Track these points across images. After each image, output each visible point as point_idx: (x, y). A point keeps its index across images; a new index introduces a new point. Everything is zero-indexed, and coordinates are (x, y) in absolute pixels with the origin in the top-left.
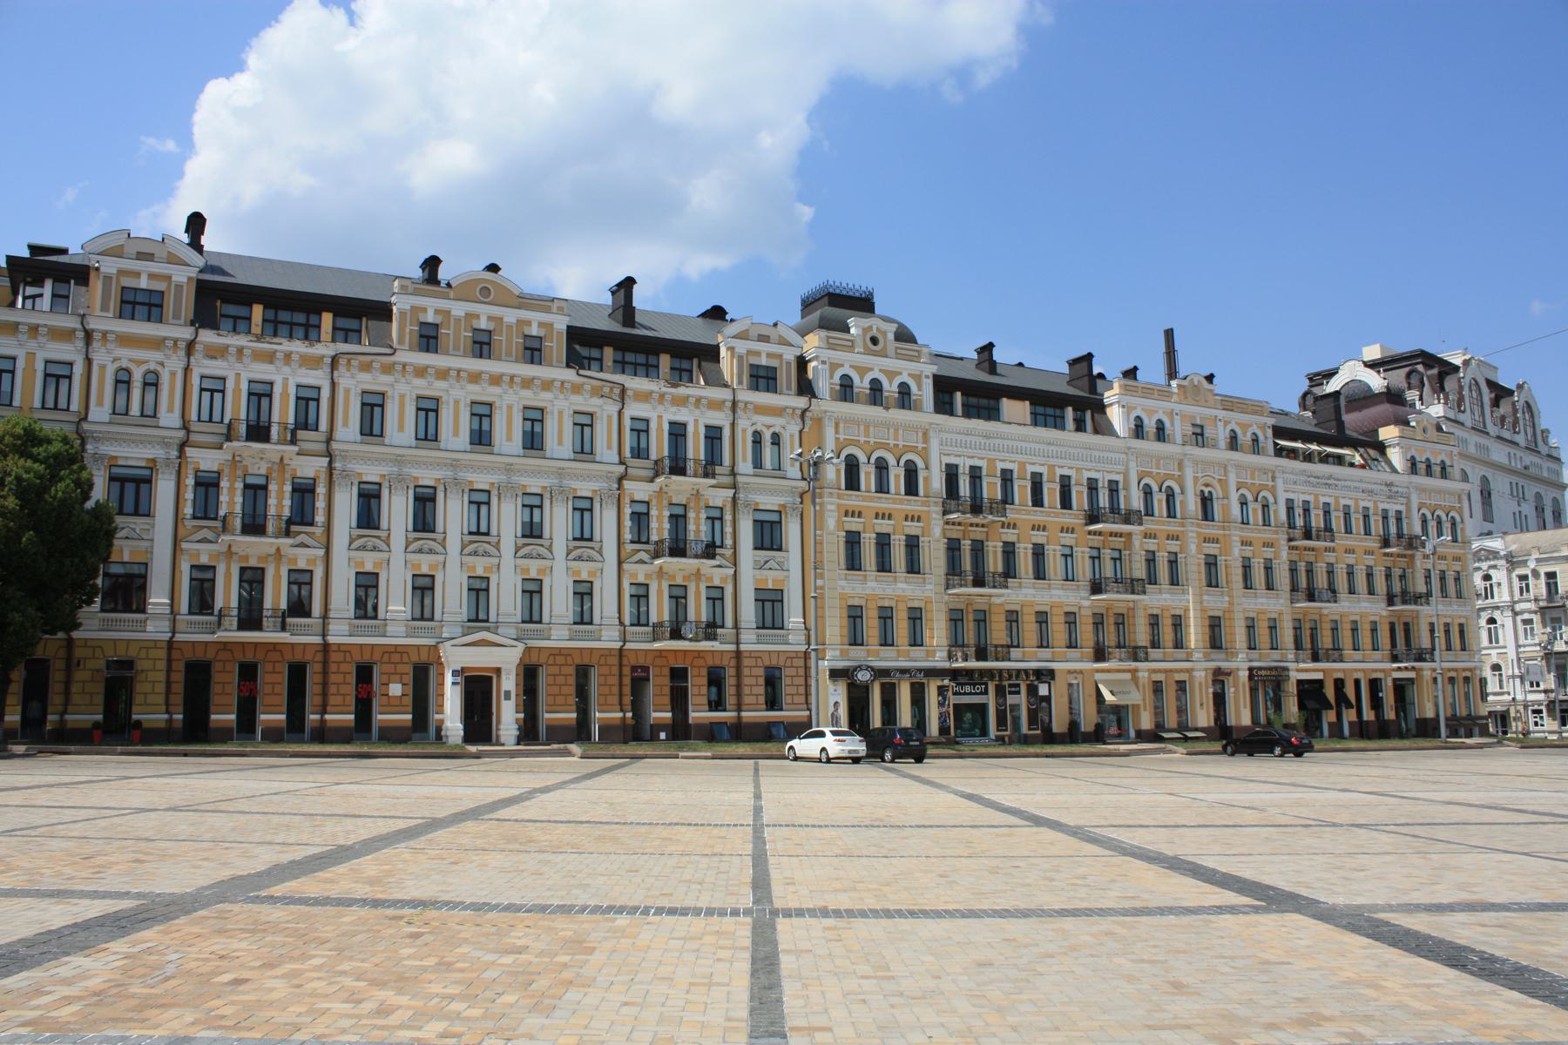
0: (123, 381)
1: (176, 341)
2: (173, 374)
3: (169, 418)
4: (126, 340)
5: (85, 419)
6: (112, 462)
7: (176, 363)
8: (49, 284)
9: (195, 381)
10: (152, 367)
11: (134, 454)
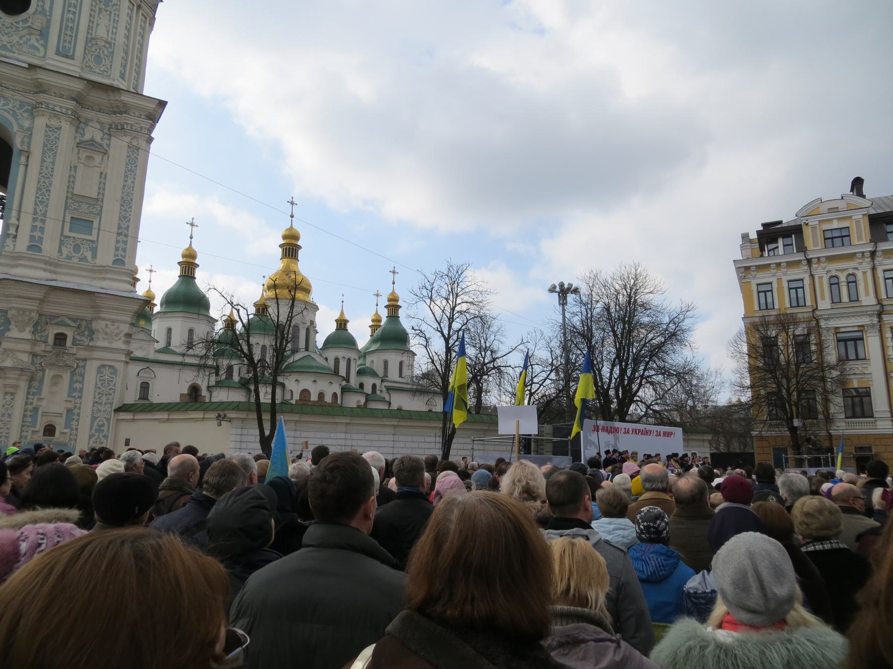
0: (834, 283)
1: (863, 253)
2: (865, 273)
4: (830, 259)
5: (816, 309)
6: (837, 330)
7: (866, 265)
8: (780, 241)
9: (880, 274)
10: (851, 271)
11: (848, 324)
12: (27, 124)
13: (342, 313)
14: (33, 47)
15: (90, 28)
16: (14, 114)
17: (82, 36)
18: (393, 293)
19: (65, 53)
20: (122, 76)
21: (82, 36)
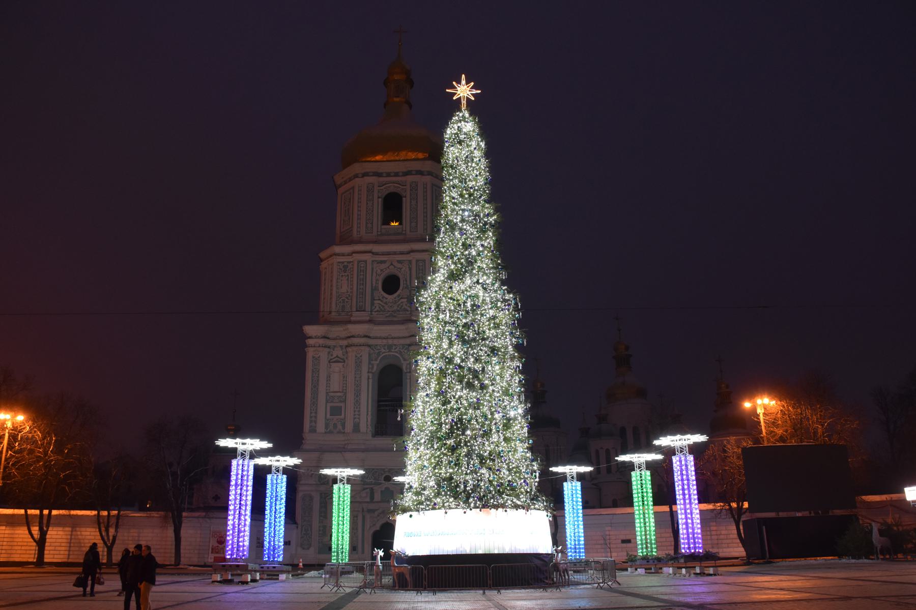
16: (401, 353)
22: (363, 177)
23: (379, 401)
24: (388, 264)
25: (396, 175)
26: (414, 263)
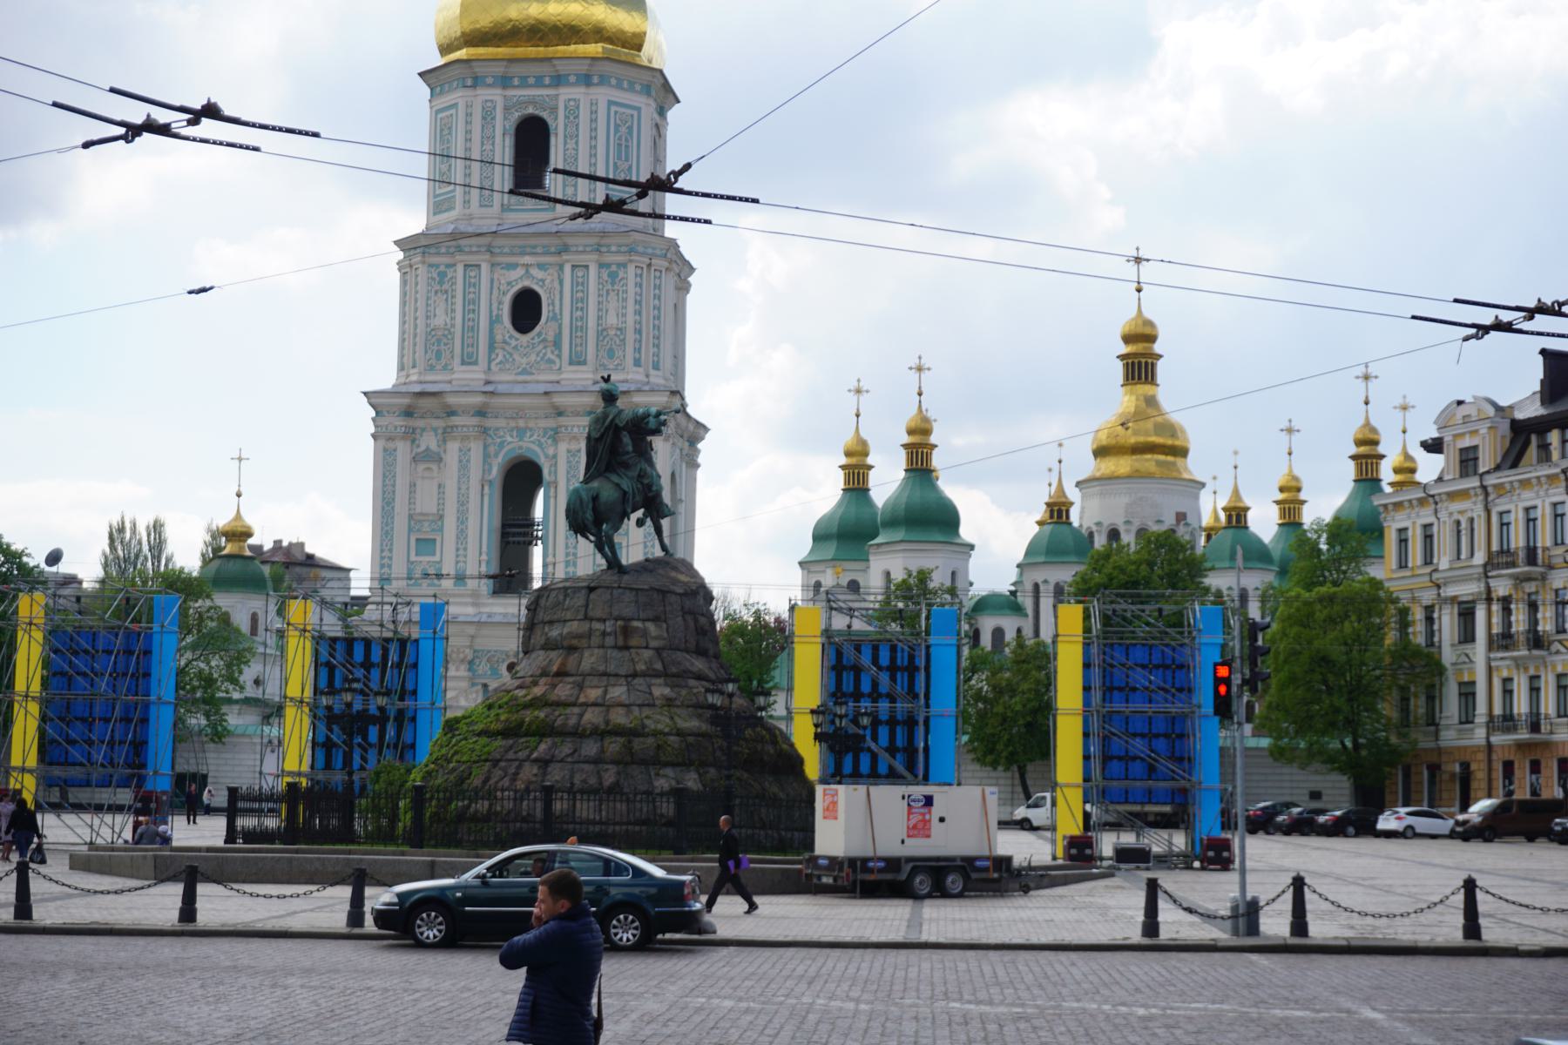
3: (1480, 558)
6: (1453, 600)
7: (1478, 511)
9: (1495, 519)
12: (551, 451)
13: (1236, 492)
14: (550, 361)
15: (599, 318)
16: (540, 445)
17: (592, 334)
18: (1367, 424)
19: (577, 361)
20: (637, 363)
21: (592, 334)
22: (474, 86)
23: (504, 526)
24: (520, 272)
25: (539, 83)
26: (567, 269)
